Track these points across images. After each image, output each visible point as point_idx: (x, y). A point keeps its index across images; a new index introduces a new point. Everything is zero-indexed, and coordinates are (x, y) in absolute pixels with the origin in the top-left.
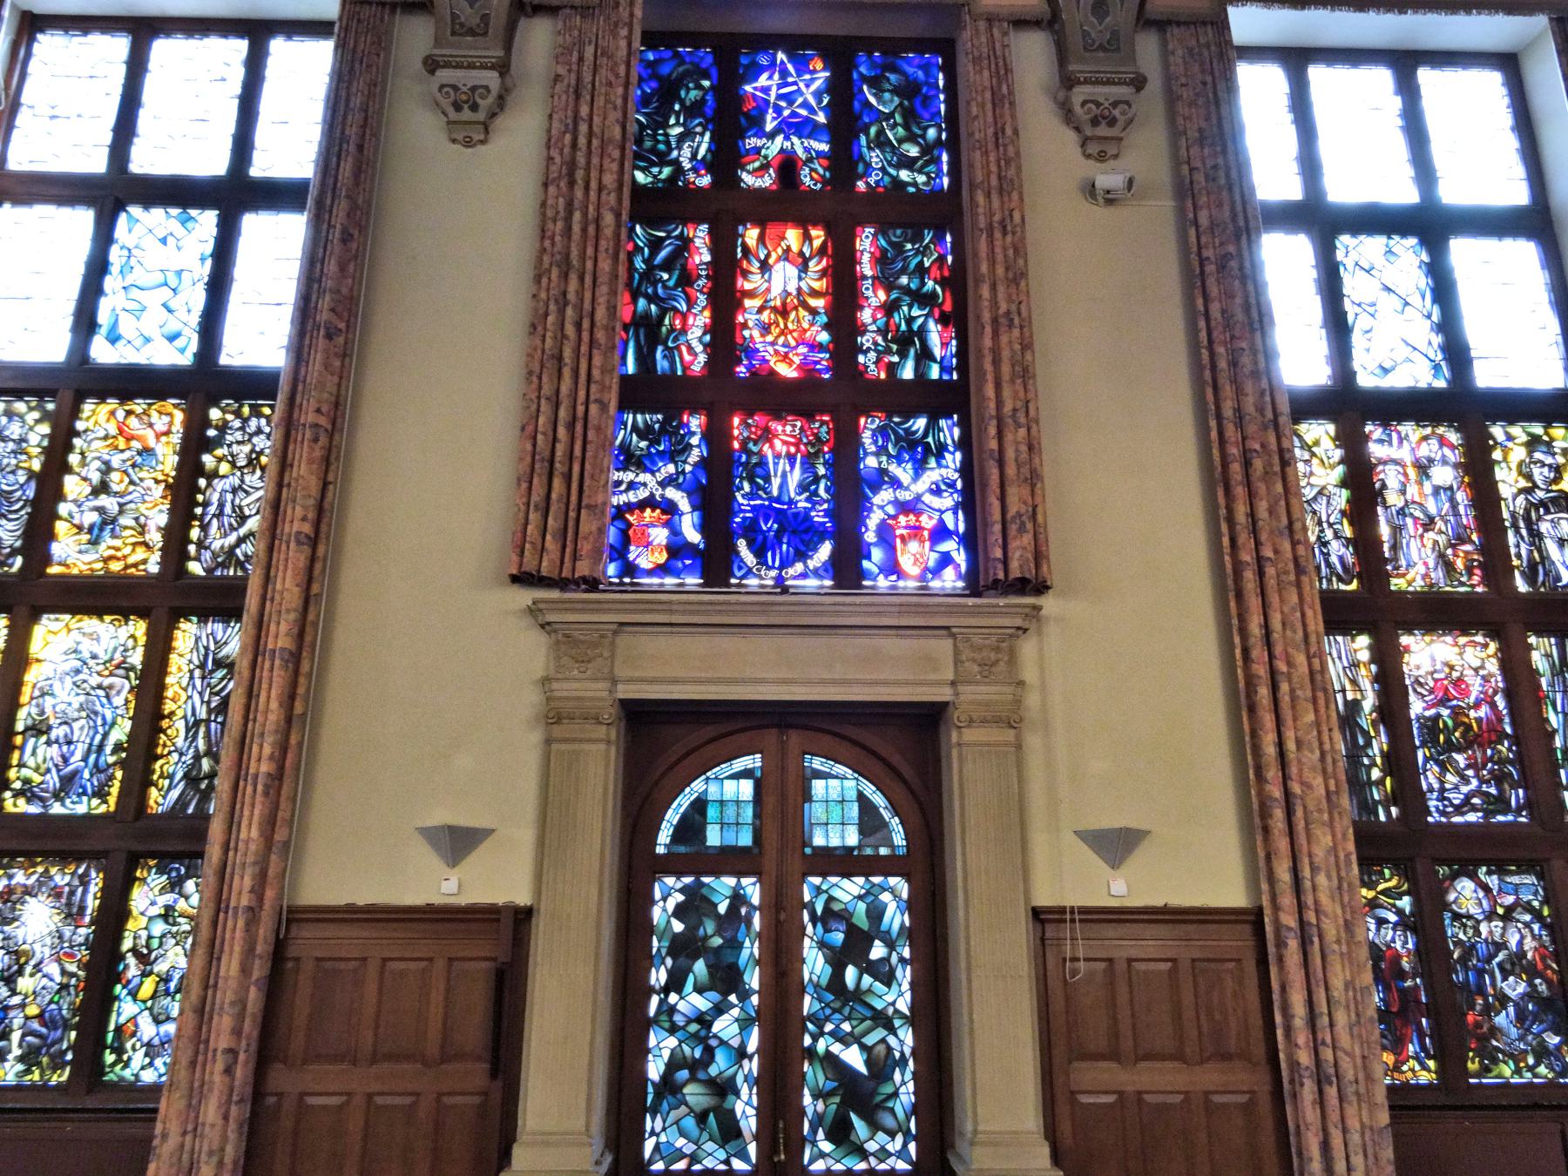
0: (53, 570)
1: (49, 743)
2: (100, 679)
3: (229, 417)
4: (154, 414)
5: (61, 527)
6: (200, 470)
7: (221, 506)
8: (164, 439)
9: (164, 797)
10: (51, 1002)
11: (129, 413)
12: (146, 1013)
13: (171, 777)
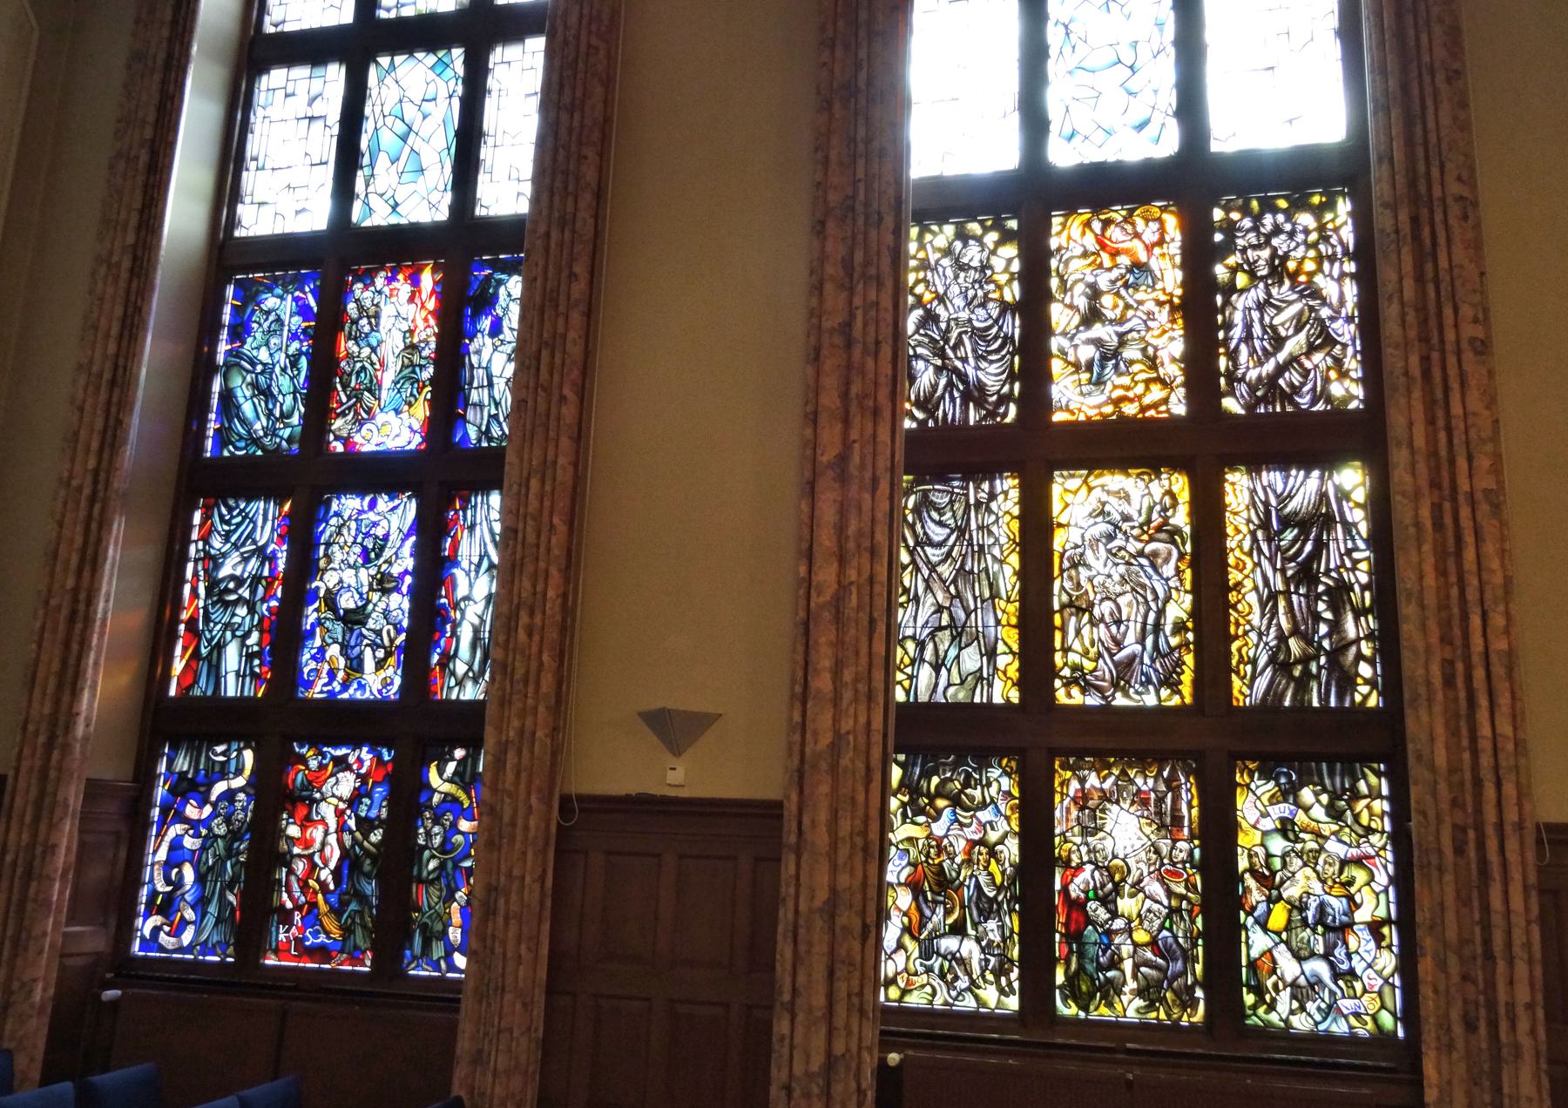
0: (1058, 417)
1: (1093, 623)
2: (1140, 546)
3: (1235, 216)
4: (1140, 223)
5: (1057, 366)
6: (1212, 286)
7: (1248, 327)
8: (1157, 251)
9: (1251, 687)
11: (1107, 223)
12: (1282, 947)
13: (1254, 662)
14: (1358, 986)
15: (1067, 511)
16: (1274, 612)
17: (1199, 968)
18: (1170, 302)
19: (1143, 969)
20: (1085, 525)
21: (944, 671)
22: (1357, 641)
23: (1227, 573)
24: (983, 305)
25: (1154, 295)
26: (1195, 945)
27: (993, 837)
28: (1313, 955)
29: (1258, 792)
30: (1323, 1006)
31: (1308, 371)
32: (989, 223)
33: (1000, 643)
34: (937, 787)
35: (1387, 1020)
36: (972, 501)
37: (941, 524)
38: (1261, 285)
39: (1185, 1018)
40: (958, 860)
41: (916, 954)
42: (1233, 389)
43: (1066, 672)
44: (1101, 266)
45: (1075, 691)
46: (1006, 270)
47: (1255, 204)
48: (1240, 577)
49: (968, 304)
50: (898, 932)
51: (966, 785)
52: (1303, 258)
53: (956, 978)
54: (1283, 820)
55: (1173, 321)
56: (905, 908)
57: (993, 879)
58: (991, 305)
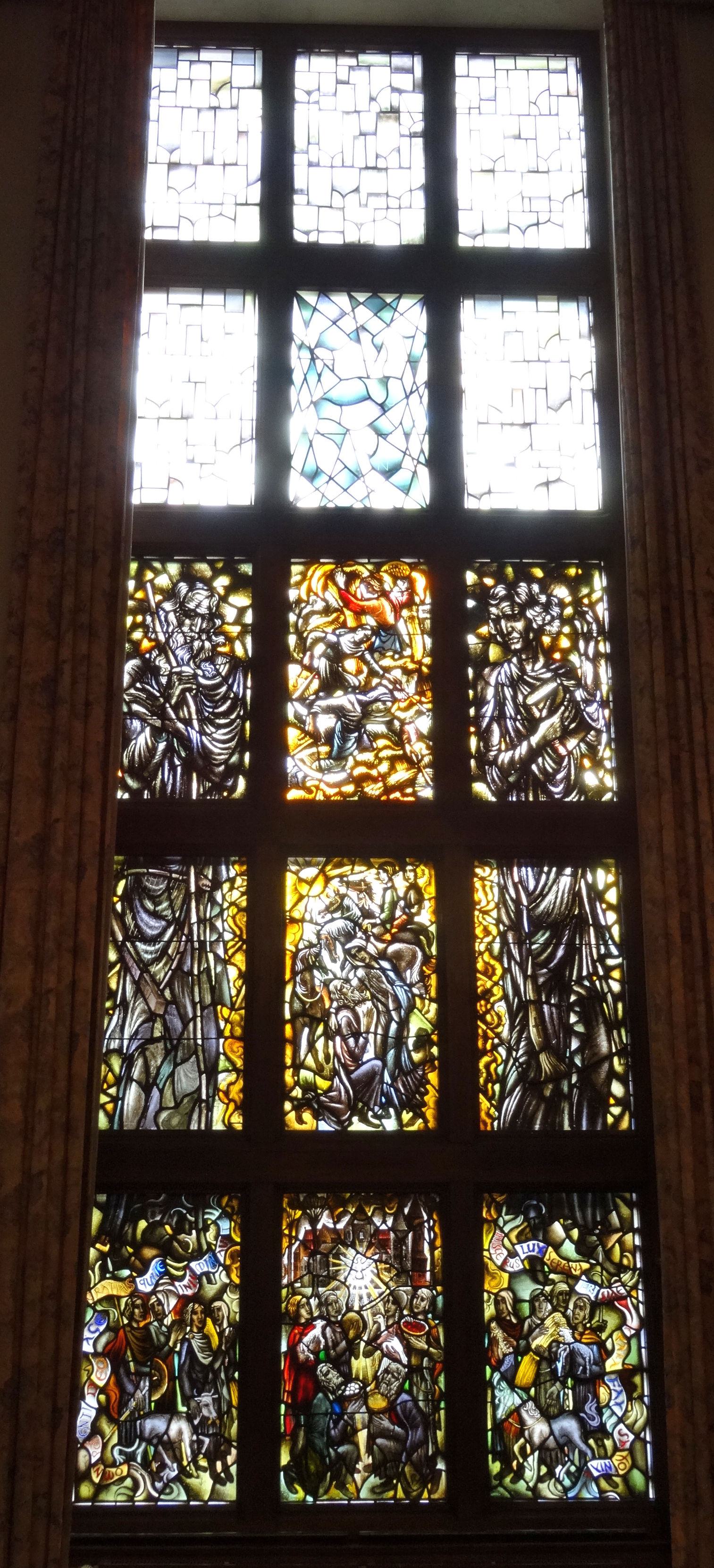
0: (293, 795)
1: (329, 1035)
2: (381, 946)
3: (489, 581)
4: (387, 579)
5: (293, 735)
6: (464, 656)
7: (500, 704)
8: (405, 613)
9: (499, 1108)
10: (401, 1390)
11: (352, 577)
12: (530, 1404)
13: (502, 1080)
14: (608, 1443)
15: (301, 906)
16: (525, 1026)
17: (440, 1434)
18: (419, 671)
19: (379, 1441)
20: (321, 921)
21: (155, 1093)
22: (609, 1057)
23: (476, 980)
24: (211, 660)
25: (400, 662)
26: (437, 1409)
27: (210, 1290)
28: (562, 1412)
29: (506, 1229)
30: (573, 1469)
31: (562, 758)
32: (220, 565)
33: (222, 1057)
34: (144, 1231)
35: (637, 1477)
36: (193, 889)
37: (155, 915)
38: (515, 660)
39: (426, 1495)
40: (168, 1321)
41: (115, 1440)
42: (484, 773)
43: (297, 1093)
44: (344, 625)
45: (307, 1116)
46: (238, 621)
47: (510, 570)
48: (489, 984)
49: (193, 657)
50: (93, 1413)
51: (179, 1229)
52: (559, 633)
53: (163, 1466)
54: (531, 1259)
55: (421, 693)
56: (101, 1384)
57: (209, 1343)
58: (220, 660)
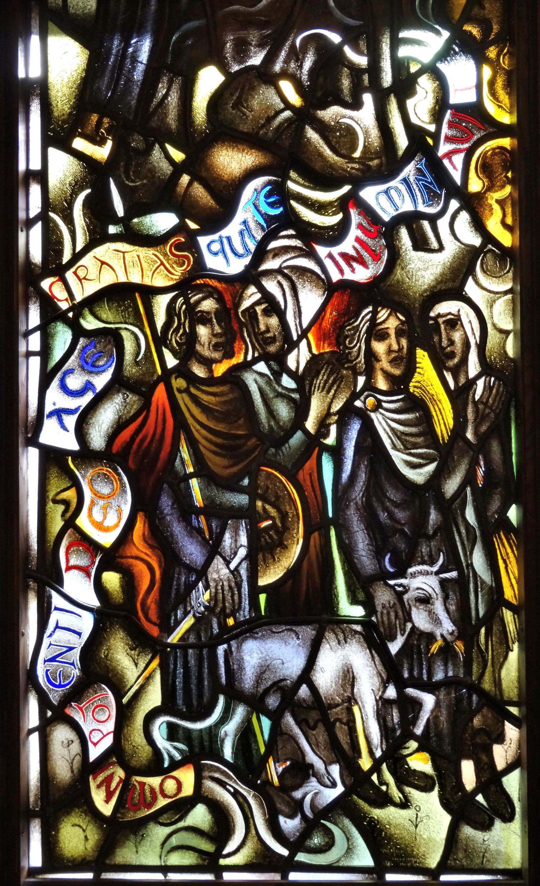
40: (298, 358)
41: (154, 697)
50: (86, 623)
53: (301, 771)
56: (107, 540)
57: (426, 420)
